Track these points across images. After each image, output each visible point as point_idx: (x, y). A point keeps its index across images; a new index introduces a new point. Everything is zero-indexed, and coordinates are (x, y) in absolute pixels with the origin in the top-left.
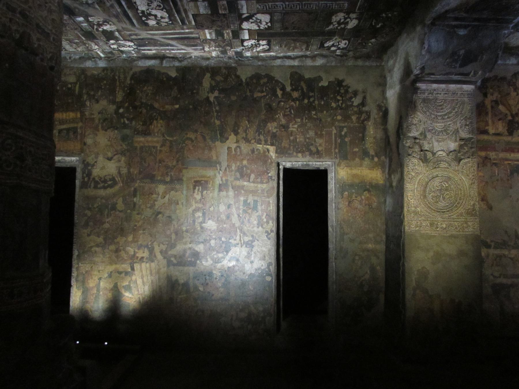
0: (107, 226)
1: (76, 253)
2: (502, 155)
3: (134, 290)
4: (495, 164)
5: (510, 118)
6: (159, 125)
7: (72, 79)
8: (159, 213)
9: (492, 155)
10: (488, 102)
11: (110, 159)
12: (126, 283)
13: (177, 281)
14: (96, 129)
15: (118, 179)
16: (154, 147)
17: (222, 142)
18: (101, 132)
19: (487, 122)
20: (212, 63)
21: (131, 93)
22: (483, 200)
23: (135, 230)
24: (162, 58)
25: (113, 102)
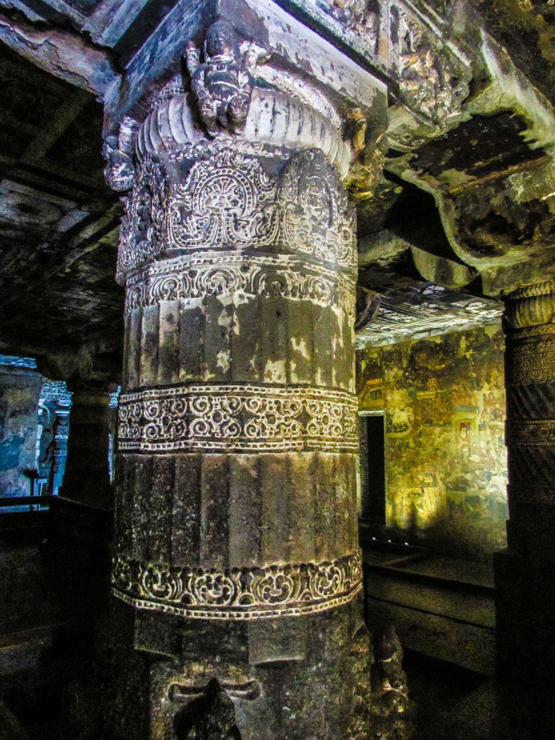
0: (404, 459)
1: (386, 479)
3: (425, 507)
6: (432, 382)
7: (375, 356)
8: (438, 449)
11: (402, 410)
12: (419, 502)
13: (454, 502)
14: (392, 389)
15: (409, 424)
16: (431, 399)
17: (479, 390)
18: (396, 391)
20: (465, 328)
21: (412, 360)
23: (422, 463)
24: (430, 330)
25: (401, 368)
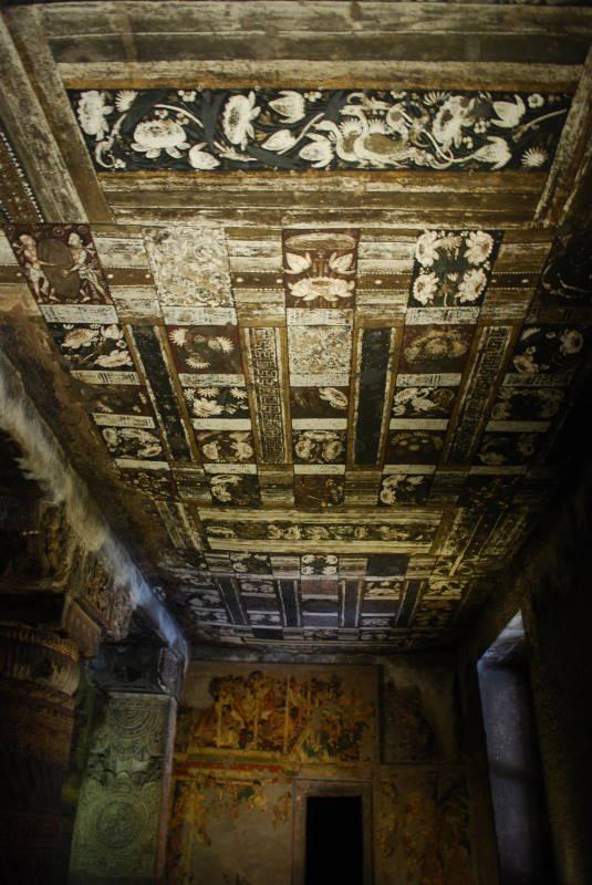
2: (230, 773)
4: (221, 785)
5: (243, 727)
9: (218, 773)
10: (218, 707)
19: (215, 731)
22: (200, 832)
